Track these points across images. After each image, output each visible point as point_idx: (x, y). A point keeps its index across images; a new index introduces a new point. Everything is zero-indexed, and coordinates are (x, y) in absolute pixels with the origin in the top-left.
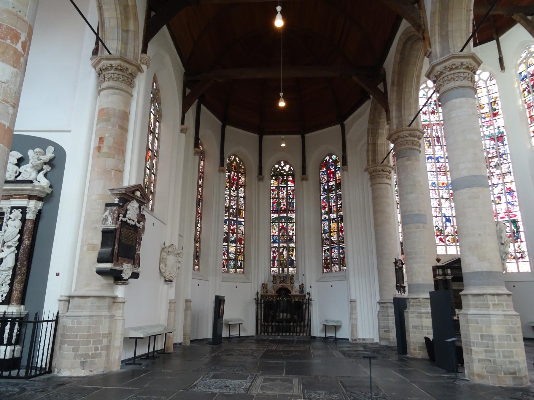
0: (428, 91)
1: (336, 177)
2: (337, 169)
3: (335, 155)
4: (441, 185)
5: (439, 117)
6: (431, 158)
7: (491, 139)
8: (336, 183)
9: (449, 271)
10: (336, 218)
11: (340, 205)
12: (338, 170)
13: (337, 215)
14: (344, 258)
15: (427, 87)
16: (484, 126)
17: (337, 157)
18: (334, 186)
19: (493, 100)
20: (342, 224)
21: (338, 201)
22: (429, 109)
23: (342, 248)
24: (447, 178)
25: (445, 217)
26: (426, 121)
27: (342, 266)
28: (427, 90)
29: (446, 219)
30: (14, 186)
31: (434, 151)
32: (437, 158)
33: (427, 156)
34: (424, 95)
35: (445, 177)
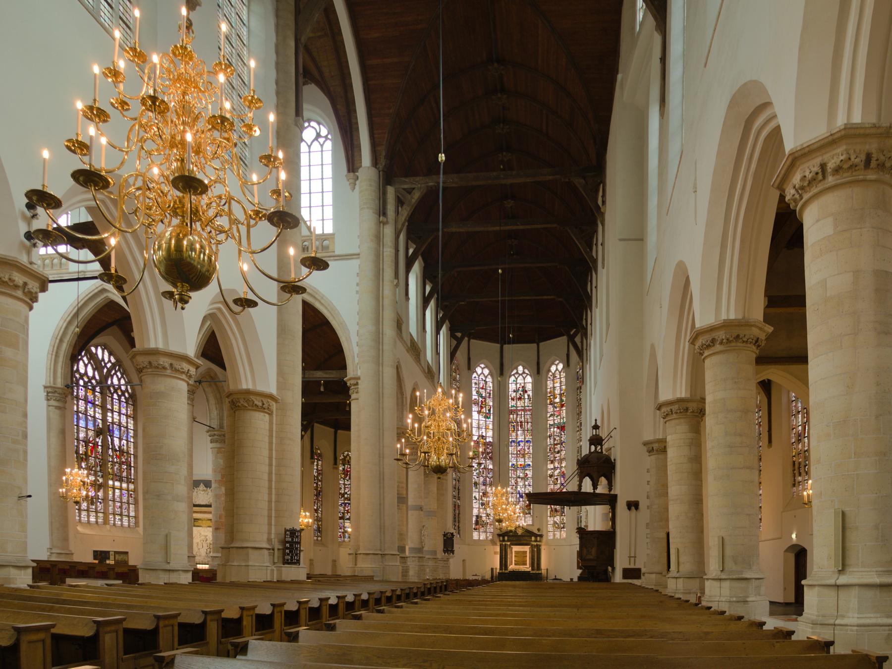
0: (518, 376)
4: (519, 466)
5: (524, 403)
6: (514, 441)
7: (558, 428)
9: (506, 538)
15: (517, 373)
16: (555, 415)
19: (562, 392)
22: (516, 394)
24: (525, 460)
25: (519, 493)
26: (514, 406)
28: (517, 376)
29: (520, 495)
31: (517, 435)
32: (519, 442)
33: (511, 440)
34: (514, 381)
35: (523, 459)
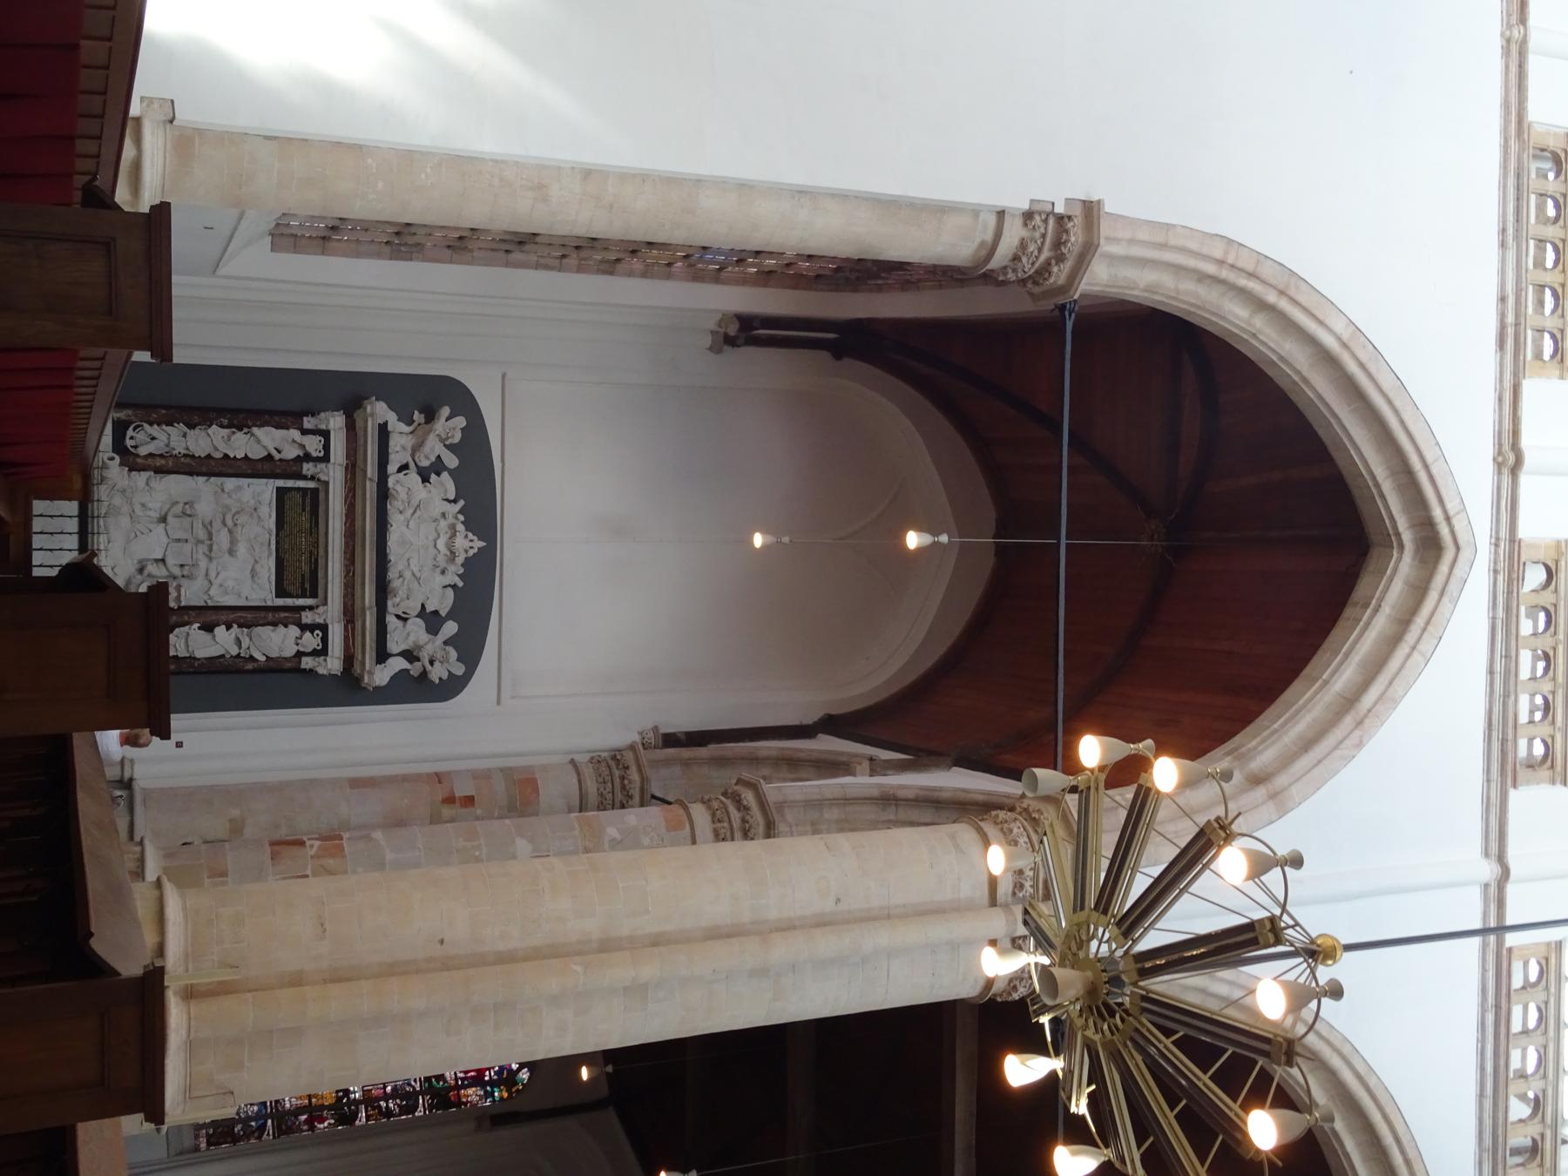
1: (466, 1087)
2: (488, 1088)
3: (530, 1078)
8: (451, 1088)
10: (349, 1098)
11: (387, 1106)
12: (486, 1091)
13: (357, 1102)
14: (235, 1140)
17: (522, 1084)
18: (441, 1083)
20: (332, 1121)
21: (398, 1101)
23: (262, 1128)
27: (211, 1131)
30: (371, 632)
